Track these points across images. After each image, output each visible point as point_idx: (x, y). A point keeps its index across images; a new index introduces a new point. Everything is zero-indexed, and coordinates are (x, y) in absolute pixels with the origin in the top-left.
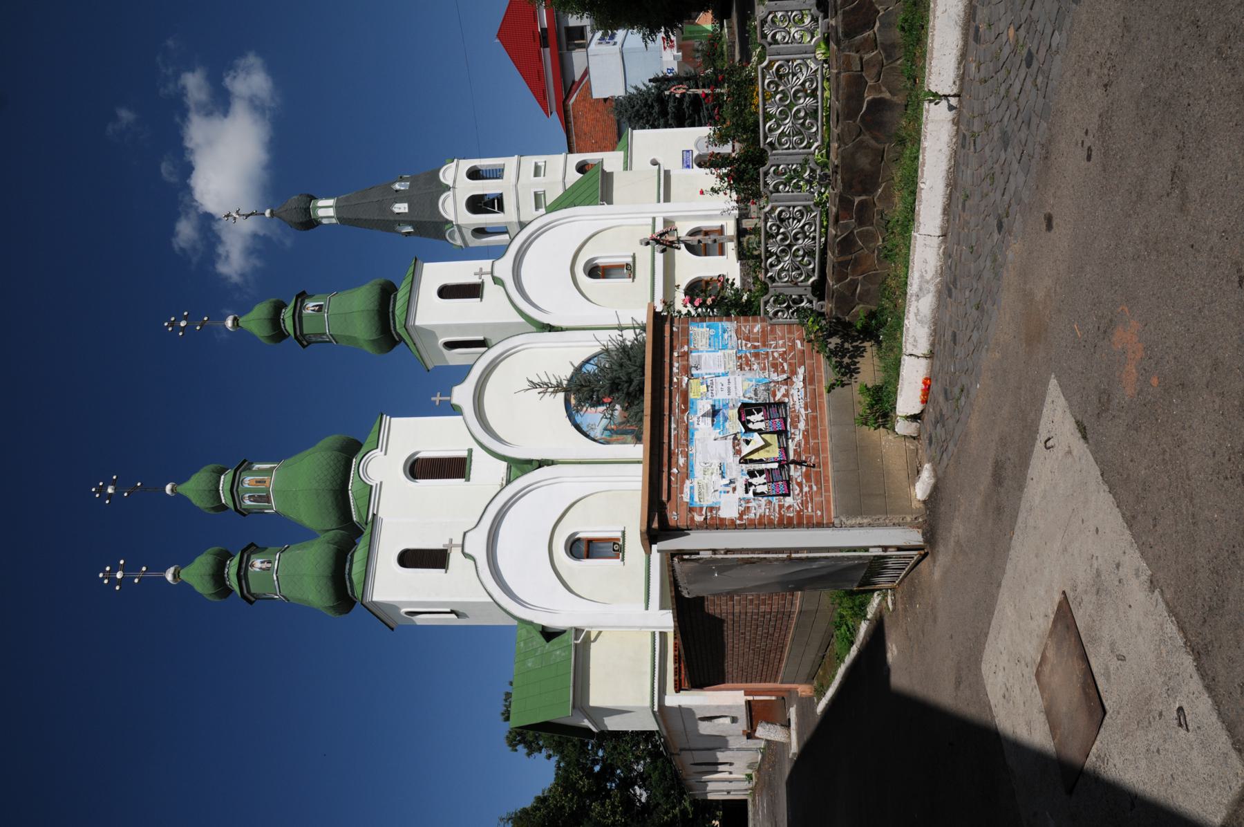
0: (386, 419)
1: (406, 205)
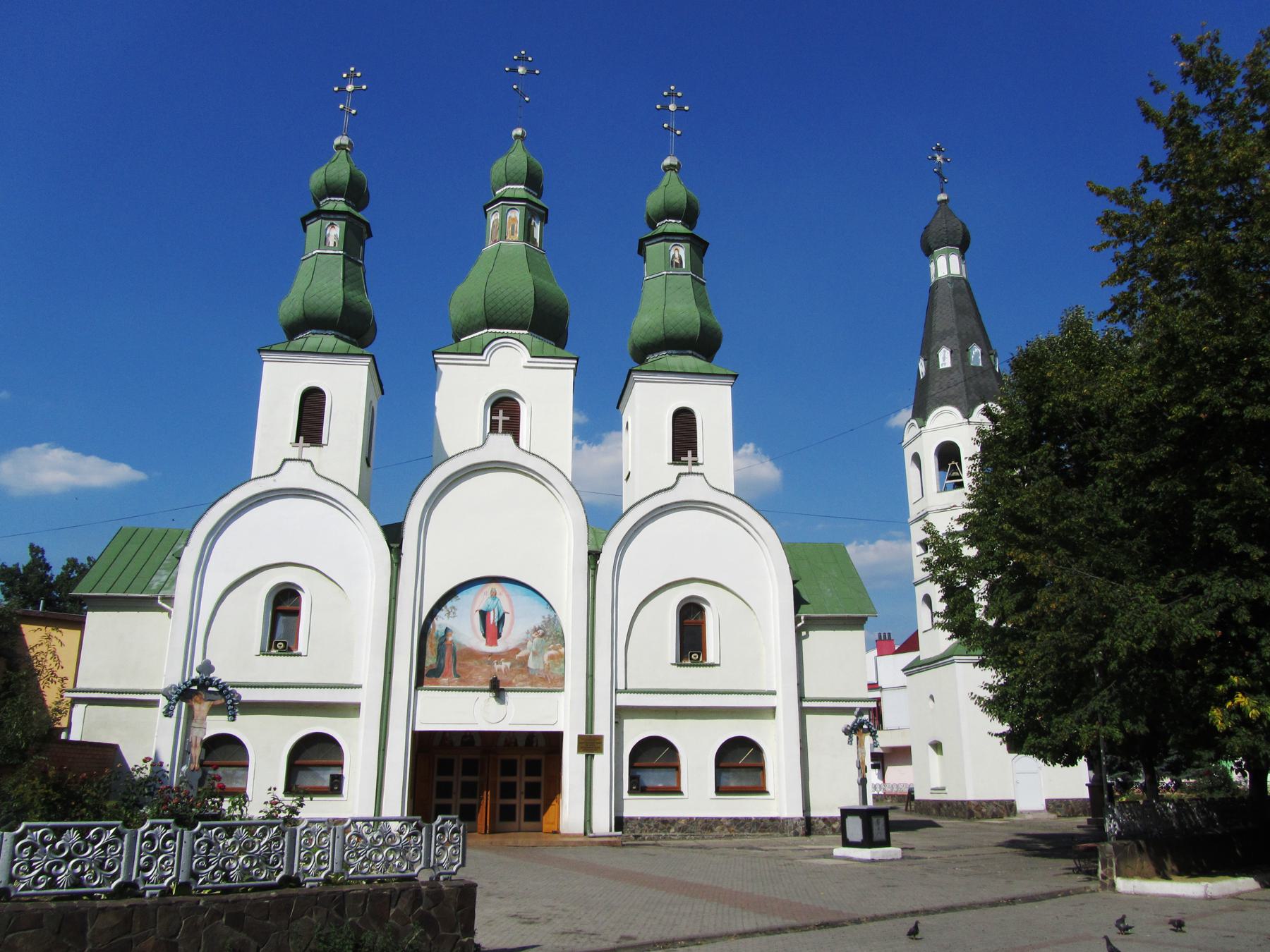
0: (572, 364)
1: (948, 365)
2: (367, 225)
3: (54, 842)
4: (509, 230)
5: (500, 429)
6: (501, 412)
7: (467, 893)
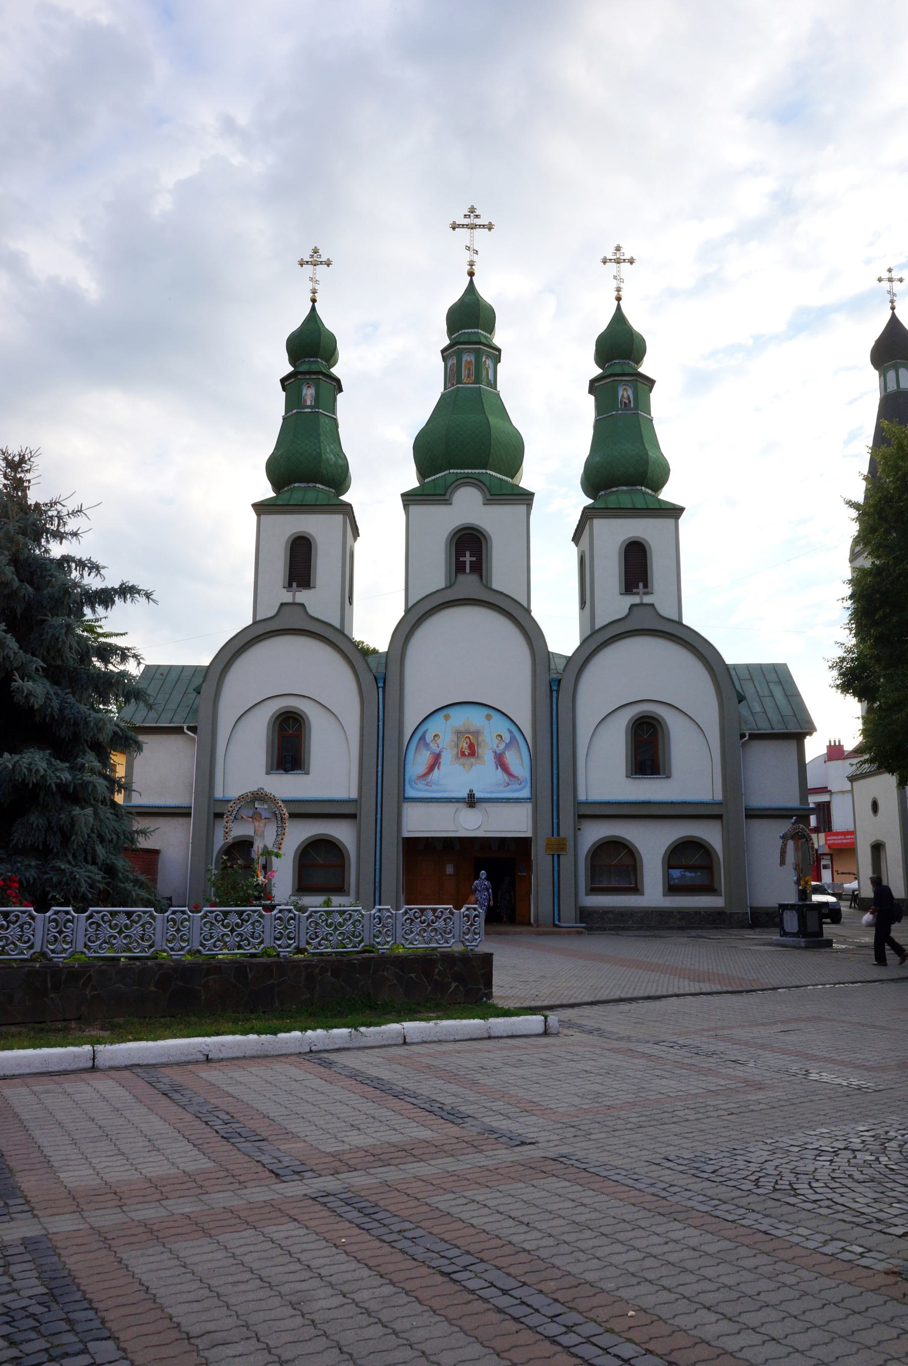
2: (338, 381)
3: (223, 920)
4: (464, 373)
5: (468, 570)
6: (468, 553)
7: (487, 960)
